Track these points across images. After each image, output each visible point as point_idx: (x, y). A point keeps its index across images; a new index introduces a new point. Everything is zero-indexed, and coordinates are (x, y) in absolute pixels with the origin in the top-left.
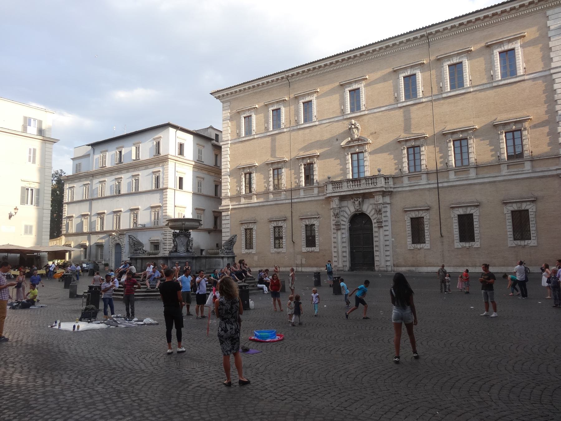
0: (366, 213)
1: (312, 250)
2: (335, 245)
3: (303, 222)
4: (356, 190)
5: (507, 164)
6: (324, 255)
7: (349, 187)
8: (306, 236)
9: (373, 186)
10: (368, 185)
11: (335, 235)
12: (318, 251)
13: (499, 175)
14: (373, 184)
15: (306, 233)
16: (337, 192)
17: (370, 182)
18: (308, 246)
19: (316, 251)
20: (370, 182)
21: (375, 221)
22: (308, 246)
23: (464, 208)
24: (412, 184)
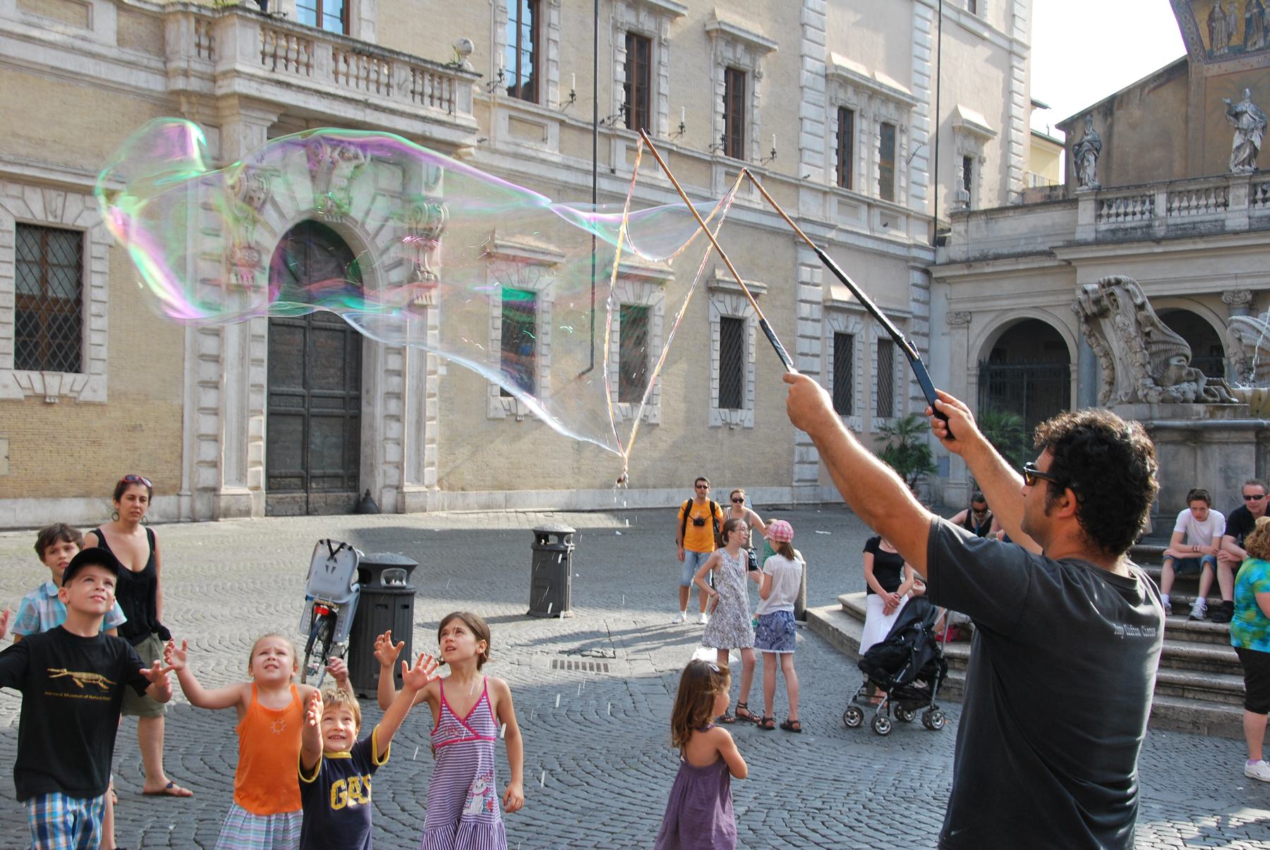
0: (358, 231)
1: (65, 391)
2: (209, 371)
3: (9, 204)
4: (377, 108)
5: (726, 169)
6: (135, 428)
7: (342, 79)
8: (19, 297)
9: (435, 112)
10: (418, 98)
12: (102, 396)
13: (708, 195)
14: (437, 102)
15: (79, 284)
16: (288, 85)
17: (428, 90)
18: (26, 357)
19: (87, 396)
20: (428, 90)
22: (26, 357)
23: (637, 285)
24: (522, 151)
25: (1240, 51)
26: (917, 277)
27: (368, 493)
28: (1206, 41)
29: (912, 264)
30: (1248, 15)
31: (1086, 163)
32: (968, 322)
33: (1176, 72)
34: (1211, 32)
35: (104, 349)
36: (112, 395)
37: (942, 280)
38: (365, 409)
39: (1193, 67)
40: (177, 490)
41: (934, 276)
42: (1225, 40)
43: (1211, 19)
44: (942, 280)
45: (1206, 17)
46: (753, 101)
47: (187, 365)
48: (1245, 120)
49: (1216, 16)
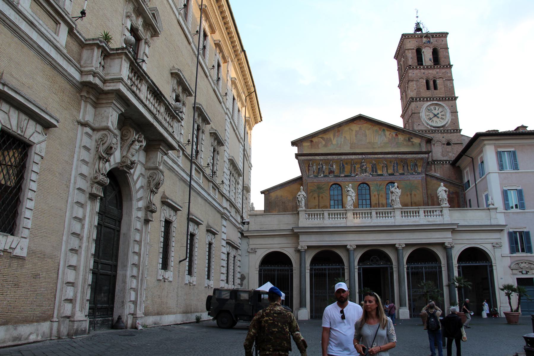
11: (79, 213)
19: (17, 252)
21: (141, 204)
25: (317, 177)
26: (239, 235)
27: (120, 318)
28: (307, 172)
29: (239, 230)
30: (319, 167)
31: (302, 201)
32: (256, 252)
33: (298, 181)
34: (309, 170)
35: (30, 222)
36: (31, 252)
37: (247, 237)
38: (120, 272)
39: (304, 179)
40: (48, 318)
41: (245, 235)
42: (313, 173)
43: (309, 166)
44: (247, 237)
45: (308, 166)
46: (217, 162)
47: (64, 238)
48: (350, 193)
49: (310, 166)
